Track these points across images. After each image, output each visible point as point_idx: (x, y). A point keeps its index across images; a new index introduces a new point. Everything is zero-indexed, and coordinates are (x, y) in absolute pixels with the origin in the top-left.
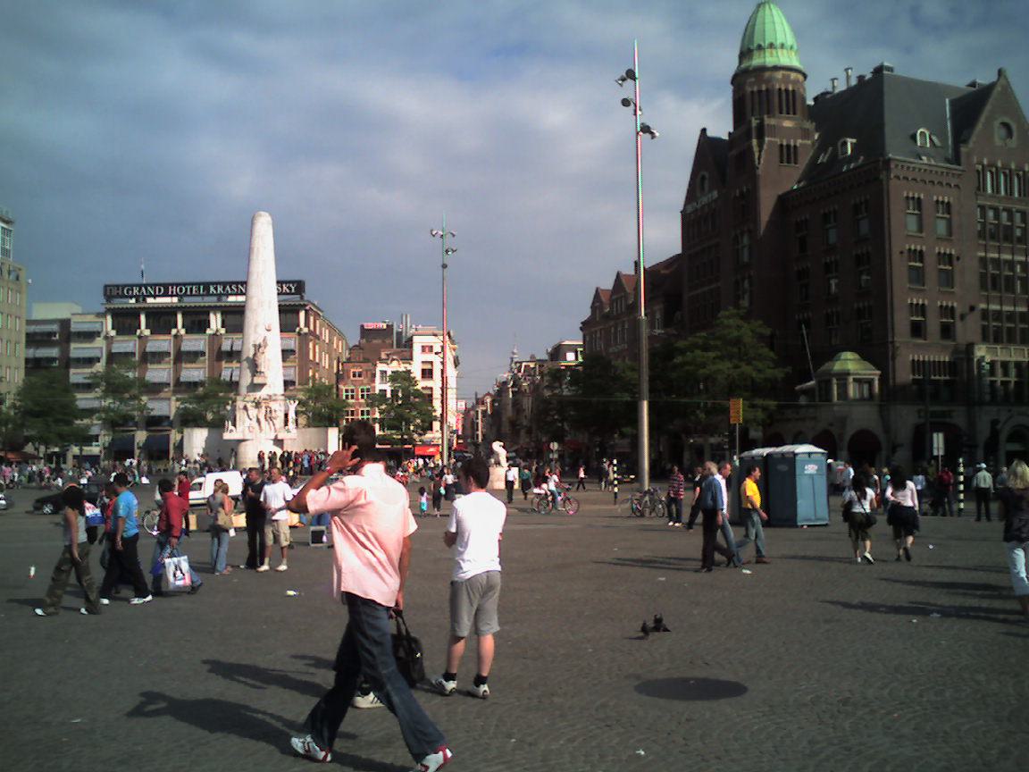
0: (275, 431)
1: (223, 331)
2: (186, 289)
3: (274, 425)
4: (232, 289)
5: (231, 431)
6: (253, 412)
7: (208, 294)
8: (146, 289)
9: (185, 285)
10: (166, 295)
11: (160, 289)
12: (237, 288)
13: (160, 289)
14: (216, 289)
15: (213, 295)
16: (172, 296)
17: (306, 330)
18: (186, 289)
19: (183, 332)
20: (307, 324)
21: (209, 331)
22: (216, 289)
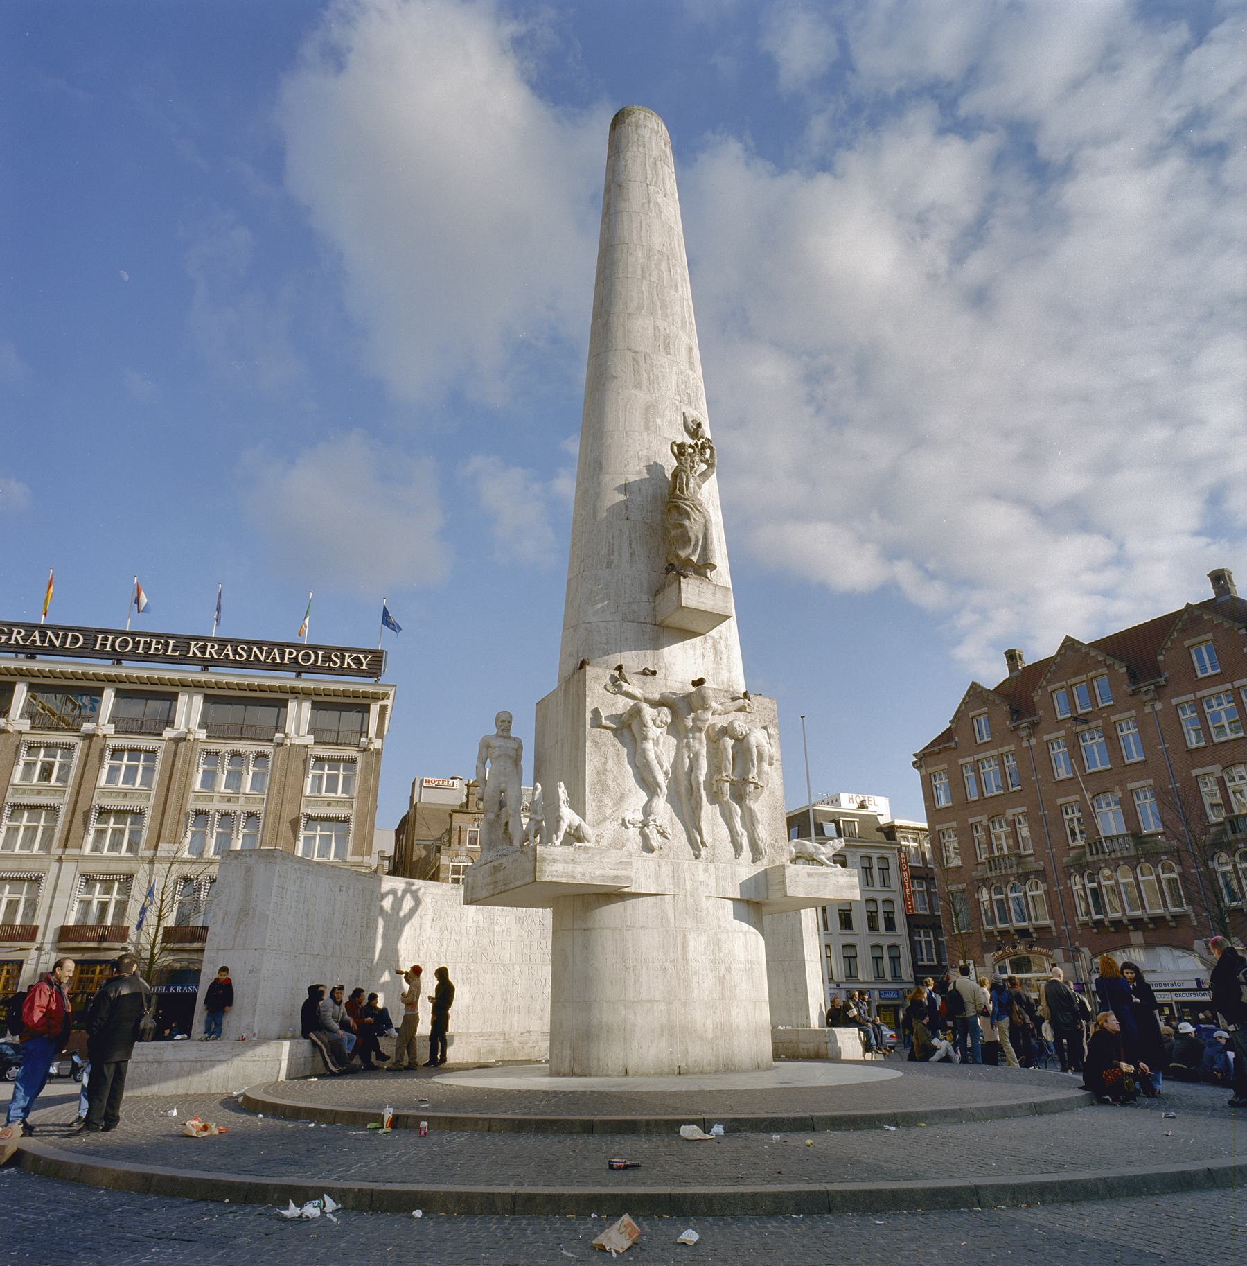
0: (757, 853)
1: (202, 734)
2: (137, 645)
3: (750, 821)
4: (235, 652)
5: (575, 836)
6: (661, 748)
7: (185, 660)
8: (43, 637)
9: (133, 634)
10: (88, 651)
11: (76, 639)
12: (249, 651)
13: (76, 639)
14: (203, 649)
15: (194, 661)
16: (102, 654)
17: (377, 744)
18: (137, 645)
19: (109, 729)
20: (380, 734)
21: (168, 733)
22: (203, 649)
